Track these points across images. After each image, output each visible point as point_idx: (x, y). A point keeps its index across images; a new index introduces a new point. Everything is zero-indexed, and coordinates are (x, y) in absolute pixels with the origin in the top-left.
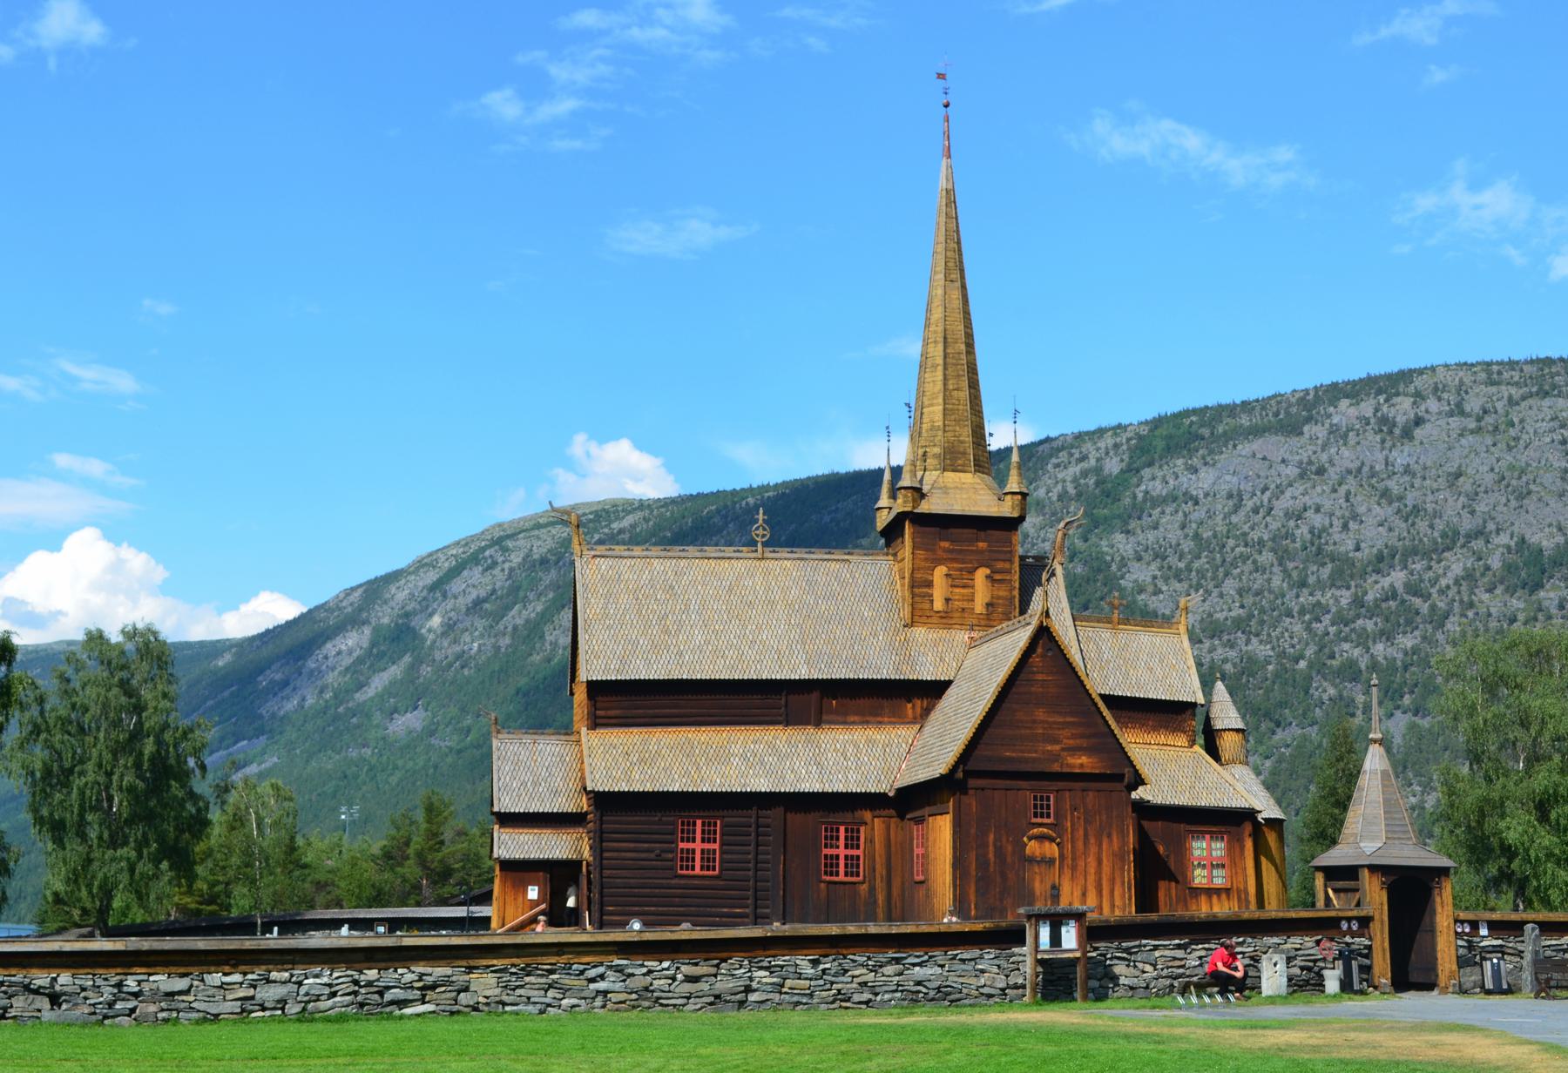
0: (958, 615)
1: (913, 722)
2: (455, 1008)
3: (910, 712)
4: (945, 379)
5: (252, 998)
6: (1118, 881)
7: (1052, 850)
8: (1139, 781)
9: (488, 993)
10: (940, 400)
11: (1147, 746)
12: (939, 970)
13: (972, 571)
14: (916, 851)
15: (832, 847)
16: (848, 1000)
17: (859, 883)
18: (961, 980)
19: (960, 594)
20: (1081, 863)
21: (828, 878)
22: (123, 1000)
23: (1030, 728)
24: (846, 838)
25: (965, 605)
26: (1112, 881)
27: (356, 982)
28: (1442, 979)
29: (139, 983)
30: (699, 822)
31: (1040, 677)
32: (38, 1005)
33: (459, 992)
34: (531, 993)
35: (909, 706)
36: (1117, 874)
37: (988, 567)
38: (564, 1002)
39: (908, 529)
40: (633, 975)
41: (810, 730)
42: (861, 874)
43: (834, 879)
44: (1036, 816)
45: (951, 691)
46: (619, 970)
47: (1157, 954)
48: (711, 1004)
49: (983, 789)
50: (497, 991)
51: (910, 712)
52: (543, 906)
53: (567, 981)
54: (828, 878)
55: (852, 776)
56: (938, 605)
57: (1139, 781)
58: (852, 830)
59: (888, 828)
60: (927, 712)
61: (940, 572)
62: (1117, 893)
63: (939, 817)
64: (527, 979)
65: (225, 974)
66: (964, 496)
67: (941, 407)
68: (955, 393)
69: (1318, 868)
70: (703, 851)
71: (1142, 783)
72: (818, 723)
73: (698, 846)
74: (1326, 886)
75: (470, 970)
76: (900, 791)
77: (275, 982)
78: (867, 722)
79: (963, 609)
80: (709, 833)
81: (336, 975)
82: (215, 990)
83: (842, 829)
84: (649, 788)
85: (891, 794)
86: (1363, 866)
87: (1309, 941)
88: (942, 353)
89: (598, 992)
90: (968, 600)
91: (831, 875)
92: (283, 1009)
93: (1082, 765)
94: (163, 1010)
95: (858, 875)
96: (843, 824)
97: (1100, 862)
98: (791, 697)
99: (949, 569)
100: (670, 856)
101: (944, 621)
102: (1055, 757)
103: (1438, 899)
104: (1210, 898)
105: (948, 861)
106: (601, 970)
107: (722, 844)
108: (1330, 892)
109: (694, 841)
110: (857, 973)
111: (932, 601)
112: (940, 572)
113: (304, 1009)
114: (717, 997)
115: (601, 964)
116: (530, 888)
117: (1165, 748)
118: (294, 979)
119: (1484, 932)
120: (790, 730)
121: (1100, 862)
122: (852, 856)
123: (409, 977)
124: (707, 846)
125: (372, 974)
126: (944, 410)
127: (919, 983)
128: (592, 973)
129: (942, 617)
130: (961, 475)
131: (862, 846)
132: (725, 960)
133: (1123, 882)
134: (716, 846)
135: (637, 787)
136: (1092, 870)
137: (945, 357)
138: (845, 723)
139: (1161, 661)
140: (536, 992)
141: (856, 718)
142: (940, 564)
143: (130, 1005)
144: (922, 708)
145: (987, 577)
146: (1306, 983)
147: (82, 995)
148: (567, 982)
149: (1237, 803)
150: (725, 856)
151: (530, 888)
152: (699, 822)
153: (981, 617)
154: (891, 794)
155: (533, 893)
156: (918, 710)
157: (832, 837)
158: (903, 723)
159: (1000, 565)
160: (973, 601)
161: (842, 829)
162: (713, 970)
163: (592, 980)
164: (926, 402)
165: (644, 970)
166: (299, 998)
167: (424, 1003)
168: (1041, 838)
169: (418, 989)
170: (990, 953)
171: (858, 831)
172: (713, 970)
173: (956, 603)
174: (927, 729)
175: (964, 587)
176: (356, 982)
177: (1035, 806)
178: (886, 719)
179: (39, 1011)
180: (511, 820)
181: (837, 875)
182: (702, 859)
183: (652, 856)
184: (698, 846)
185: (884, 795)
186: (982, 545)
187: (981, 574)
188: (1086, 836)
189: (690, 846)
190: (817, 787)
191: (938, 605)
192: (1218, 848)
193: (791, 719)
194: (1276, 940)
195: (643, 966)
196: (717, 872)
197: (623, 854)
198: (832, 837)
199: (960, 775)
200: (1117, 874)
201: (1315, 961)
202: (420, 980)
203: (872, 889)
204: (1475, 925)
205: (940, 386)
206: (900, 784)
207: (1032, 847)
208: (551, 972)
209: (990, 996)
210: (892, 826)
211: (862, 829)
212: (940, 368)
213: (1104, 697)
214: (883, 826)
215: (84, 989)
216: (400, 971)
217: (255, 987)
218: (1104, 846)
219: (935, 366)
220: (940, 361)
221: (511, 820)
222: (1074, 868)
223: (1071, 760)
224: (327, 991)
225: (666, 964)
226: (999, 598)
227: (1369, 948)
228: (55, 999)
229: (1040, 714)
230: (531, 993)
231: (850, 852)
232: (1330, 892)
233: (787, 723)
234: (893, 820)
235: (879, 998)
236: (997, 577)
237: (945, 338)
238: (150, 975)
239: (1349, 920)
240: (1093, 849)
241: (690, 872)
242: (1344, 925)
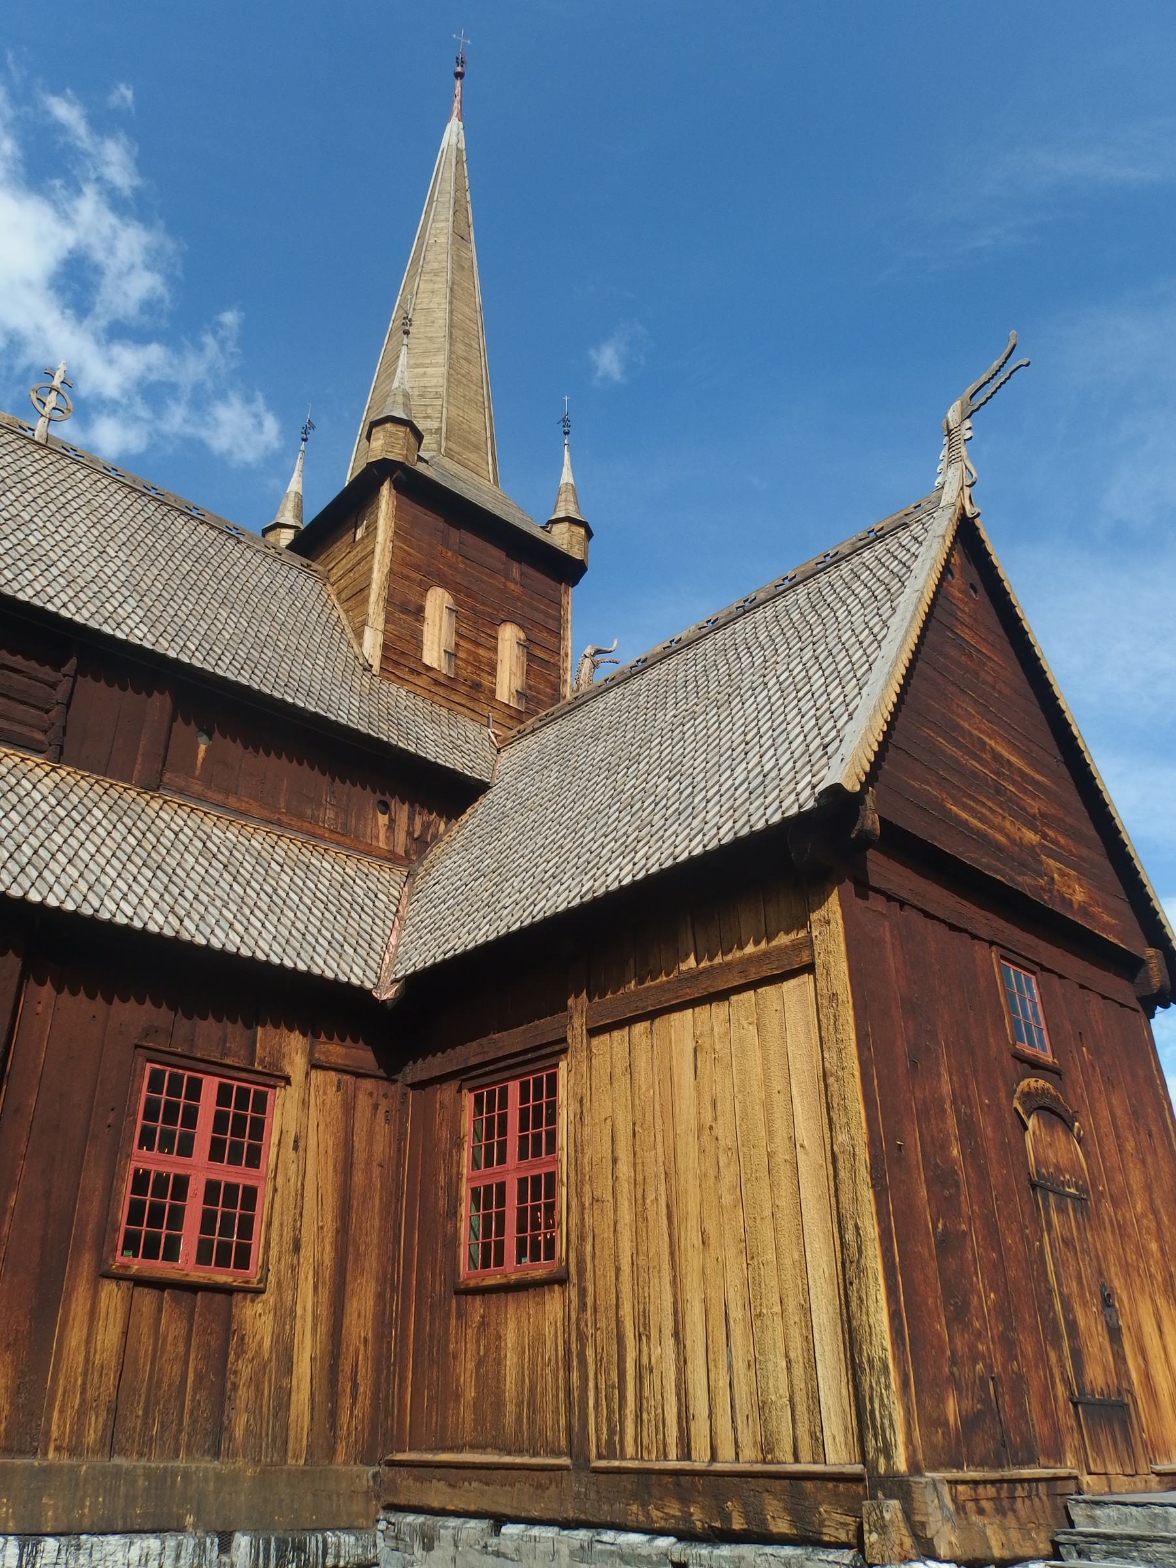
15: (167, 1142)
17: (245, 1291)
21: (138, 1265)
24: (220, 1122)
35: (383, 819)
37: (521, 627)
39: (386, 497)
42: (256, 1256)
43: (159, 1268)
49: (902, 904)
54: (138, 1265)
56: (433, 655)
58: (243, 1094)
59: (349, 1108)
60: (421, 844)
72: (152, 785)
76: (416, 984)
78: (280, 824)
83: (210, 1086)
85: (387, 994)
91: (151, 1252)
95: (243, 1261)
96: (214, 1067)
98: (87, 685)
101: (441, 691)
122: (232, 1188)
129: (437, 682)
141: (255, 809)
144: (409, 833)
154: (387, 994)
157: (171, 1111)
161: (210, 1086)
181: (172, 1254)
185: (361, 994)
187: (509, 637)
198: (171, 1111)
203: (285, 1316)
210: (363, 1102)
214: (333, 1097)
231: (226, 1173)
233: (59, 755)
234: (368, 1084)
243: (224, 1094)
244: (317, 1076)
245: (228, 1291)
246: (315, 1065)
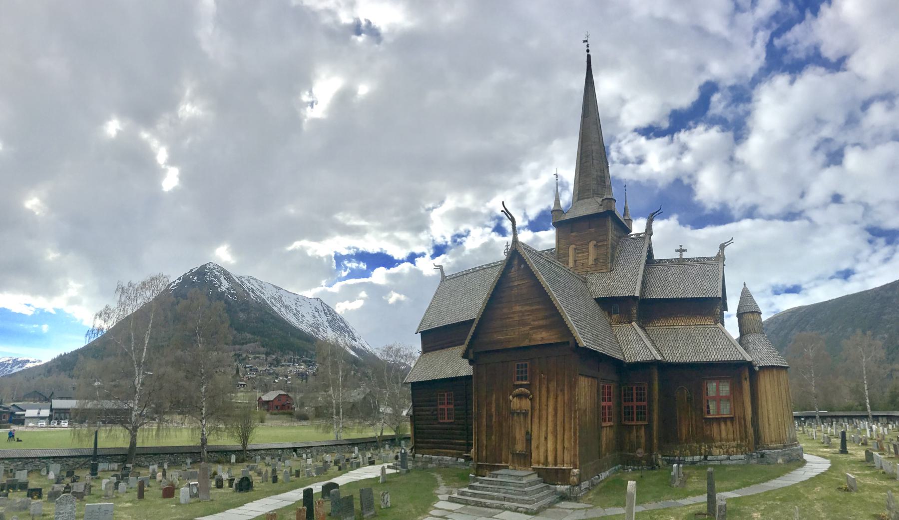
0: (580, 267)
11: (688, 327)
19: (582, 256)
37: (595, 240)
61: (572, 247)
79: (583, 264)
90: (585, 259)
99: (576, 245)
112: (572, 247)
117: (698, 326)
142: (572, 244)
153: (592, 266)
159: (601, 238)
160: (588, 258)
173: (580, 261)
186: (593, 230)
188: (548, 391)
218: (559, 399)
236: (599, 244)
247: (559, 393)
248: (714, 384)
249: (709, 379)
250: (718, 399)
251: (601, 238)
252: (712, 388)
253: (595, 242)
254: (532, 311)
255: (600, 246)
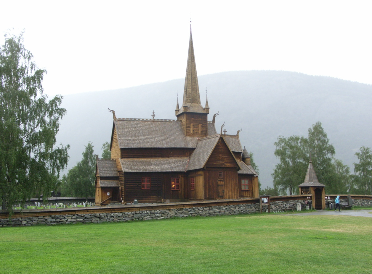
1: (187, 157)
2: (167, 217)
3: (187, 155)
4: (192, 83)
5: (133, 217)
6: (235, 189)
7: (222, 183)
8: (239, 169)
9: (172, 214)
10: (191, 88)
12: (245, 208)
13: (198, 125)
14: (191, 184)
16: (231, 214)
18: (249, 210)
20: (228, 186)
21: (173, 190)
22: (112, 218)
23: (219, 158)
25: (198, 132)
26: (234, 190)
27: (151, 213)
28: (323, 208)
29: (114, 214)
30: (146, 178)
31: (220, 148)
32: (97, 220)
33: (168, 214)
34: (179, 214)
35: (187, 153)
36: (235, 187)
37: (201, 124)
38: (185, 216)
40: (196, 210)
41: (167, 158)
44: (219, 176)
45: (196, 149)
46: (194, 209)
47: (279, 204)
48: (209, 215)
50: (174, 214)
51: (187, 155)
52: (111, 197)
53: (185, 212)
55: (177, 168)
56: (191, 132)
57: (239, 169)
61: (192, 125)
62: (235, 192)
63: (199, 177)
64: (179, 211)
65: (128, 212)
66: (197, 109)
67: (191, 89)
68: (194, 86)
69: (300, 187)
70: (147, 184)
71: (240, 169)
72: (168, 157)
73: (146, 183)
74: (301, 190)
75: (169, 210)
76: (187, 171)
77: (137, 213)
80: (148, 180)
81: (147, 212)
82: (127, 215)
84: (136, 171)
85: (186, 172)
86: (310, 187)
87: (302, 201)
88: (191, 77)
89: (190, 214)
92: (138, 219)
93: (228, 166)
94: (118, 220)
95: (178, 189)
97: (232, 185)
99: (194, 124)
100: (140, 185)
102: (223, 164)
103: (322, 193)
104: (246, 192)
105: (202, 186)
106: (190, 209)
107: (151, 183)
108: (302, 192)
109: (145, 182)
110: (232, 208)
111: (190, 131)
112: (192, 125)
113: (143, 218)
114: (210, 214)
115: (191, 208)
116: (108, 193)
118: (140, 213)
119: (329, 198)
120: (163, 158)
121: (232, 185)
123: (159, 212)
124: (148, 183)
125: (153, 211)
126: (192, 90)
127: (242, 210)
128: (189, 210)
129: (192, 134)
130: (195, 104)
131: (179, 183)
132: (210, 207)
133: (236, 190)
134: (150, 183)
135: (134, 171)
136: (230, 187)
137: (192, 78)
138: (174, 157)
139: (234, 143)
140: (180, 214)
141: (176, 156)
143: (113, 219)
145: (202, 126)
146: (304, 208)
147: (105, 217)
148: (185, 212)
149: (251, 173)
150: (152, 185)
151: (108, 193)
152: (146, 178)
154: (186, 172)
155: (108, 194)
156: (189, 154)
158: (185, 157)
159: (204, 123)
160: (198, 131)
162: (209, 209)
163: (189, 211)
164: (188, 88)
165: (198, 209)
166: (142, 216)
167: (162, 217)
168: (221, 181)
169: (161, 214)
170: (253, 204)
171: (178, 180)
172: (209, 209)
174: (192, 158)
175: (197, 128)
176: (151, 213)
177: (219, 174)
178: (182, 156)
179: (97, 221)
180: (102, 178)
182: (147, 186)
183: (136, 185)
184: (146, 183)
186: (200, 119)
187: (200, 125)
188: (229, 180)
189: (144, 183)
190: (170, 171)
191: (191, 132)
192: (247, 182)
193: (162, 156)
194: (297, 201)
195: (197, 208)
196: (150, 189)
197: (130, 185)
199: (205, 168)
200: (235, 187)
201: (303, 204)
202: (161, 212)
204: (328, 197)
205: (191, 84)
206: (187, 170)
207: (219, 183)
208: (182, 210)
209: (253, 212)
211: (179, 179)
212: (191, 81)
213: (233, 152)
215: (104, 216)
216: (158, 210)
217: (133, 214)
219: (189, 80)
220: (190, 79)
221: (102, 178)
222: (227, 187)
223: (226, 165)
224: (146, 215)
225: (201, 208)
226: (204, 130)
227: (312, 202)
228: (100, 218)
229: (220, 156)
230: (179, 214)
232: (302, 192)
235: (235, 213)
236: (203, 126)
237: (192, 74)
238: (115, 213)
239: (308, 197)
240: (230, 183)
241: (144, 189)
242: (308, 198)
243: (176, 179)
244: (182, 177)
245: (178, 190)
246: (182, 177)
247: (233, 181)
248: (244, 180)
249: (242, 179)
250: (245, 185)
251: (204, 123)
252: (243, 182)
253: (201, 125)
254: (227, 157)
255: (204, 127)
